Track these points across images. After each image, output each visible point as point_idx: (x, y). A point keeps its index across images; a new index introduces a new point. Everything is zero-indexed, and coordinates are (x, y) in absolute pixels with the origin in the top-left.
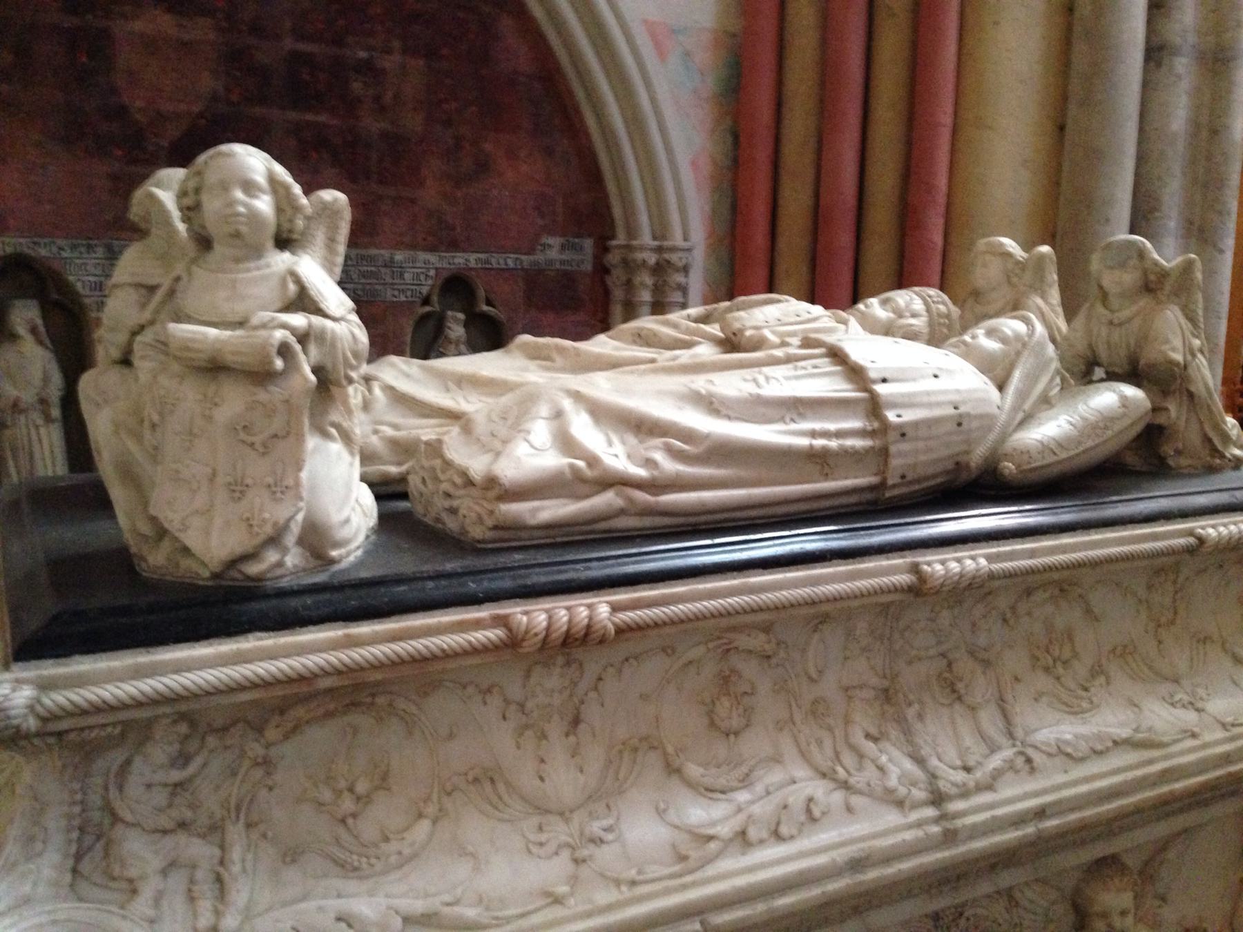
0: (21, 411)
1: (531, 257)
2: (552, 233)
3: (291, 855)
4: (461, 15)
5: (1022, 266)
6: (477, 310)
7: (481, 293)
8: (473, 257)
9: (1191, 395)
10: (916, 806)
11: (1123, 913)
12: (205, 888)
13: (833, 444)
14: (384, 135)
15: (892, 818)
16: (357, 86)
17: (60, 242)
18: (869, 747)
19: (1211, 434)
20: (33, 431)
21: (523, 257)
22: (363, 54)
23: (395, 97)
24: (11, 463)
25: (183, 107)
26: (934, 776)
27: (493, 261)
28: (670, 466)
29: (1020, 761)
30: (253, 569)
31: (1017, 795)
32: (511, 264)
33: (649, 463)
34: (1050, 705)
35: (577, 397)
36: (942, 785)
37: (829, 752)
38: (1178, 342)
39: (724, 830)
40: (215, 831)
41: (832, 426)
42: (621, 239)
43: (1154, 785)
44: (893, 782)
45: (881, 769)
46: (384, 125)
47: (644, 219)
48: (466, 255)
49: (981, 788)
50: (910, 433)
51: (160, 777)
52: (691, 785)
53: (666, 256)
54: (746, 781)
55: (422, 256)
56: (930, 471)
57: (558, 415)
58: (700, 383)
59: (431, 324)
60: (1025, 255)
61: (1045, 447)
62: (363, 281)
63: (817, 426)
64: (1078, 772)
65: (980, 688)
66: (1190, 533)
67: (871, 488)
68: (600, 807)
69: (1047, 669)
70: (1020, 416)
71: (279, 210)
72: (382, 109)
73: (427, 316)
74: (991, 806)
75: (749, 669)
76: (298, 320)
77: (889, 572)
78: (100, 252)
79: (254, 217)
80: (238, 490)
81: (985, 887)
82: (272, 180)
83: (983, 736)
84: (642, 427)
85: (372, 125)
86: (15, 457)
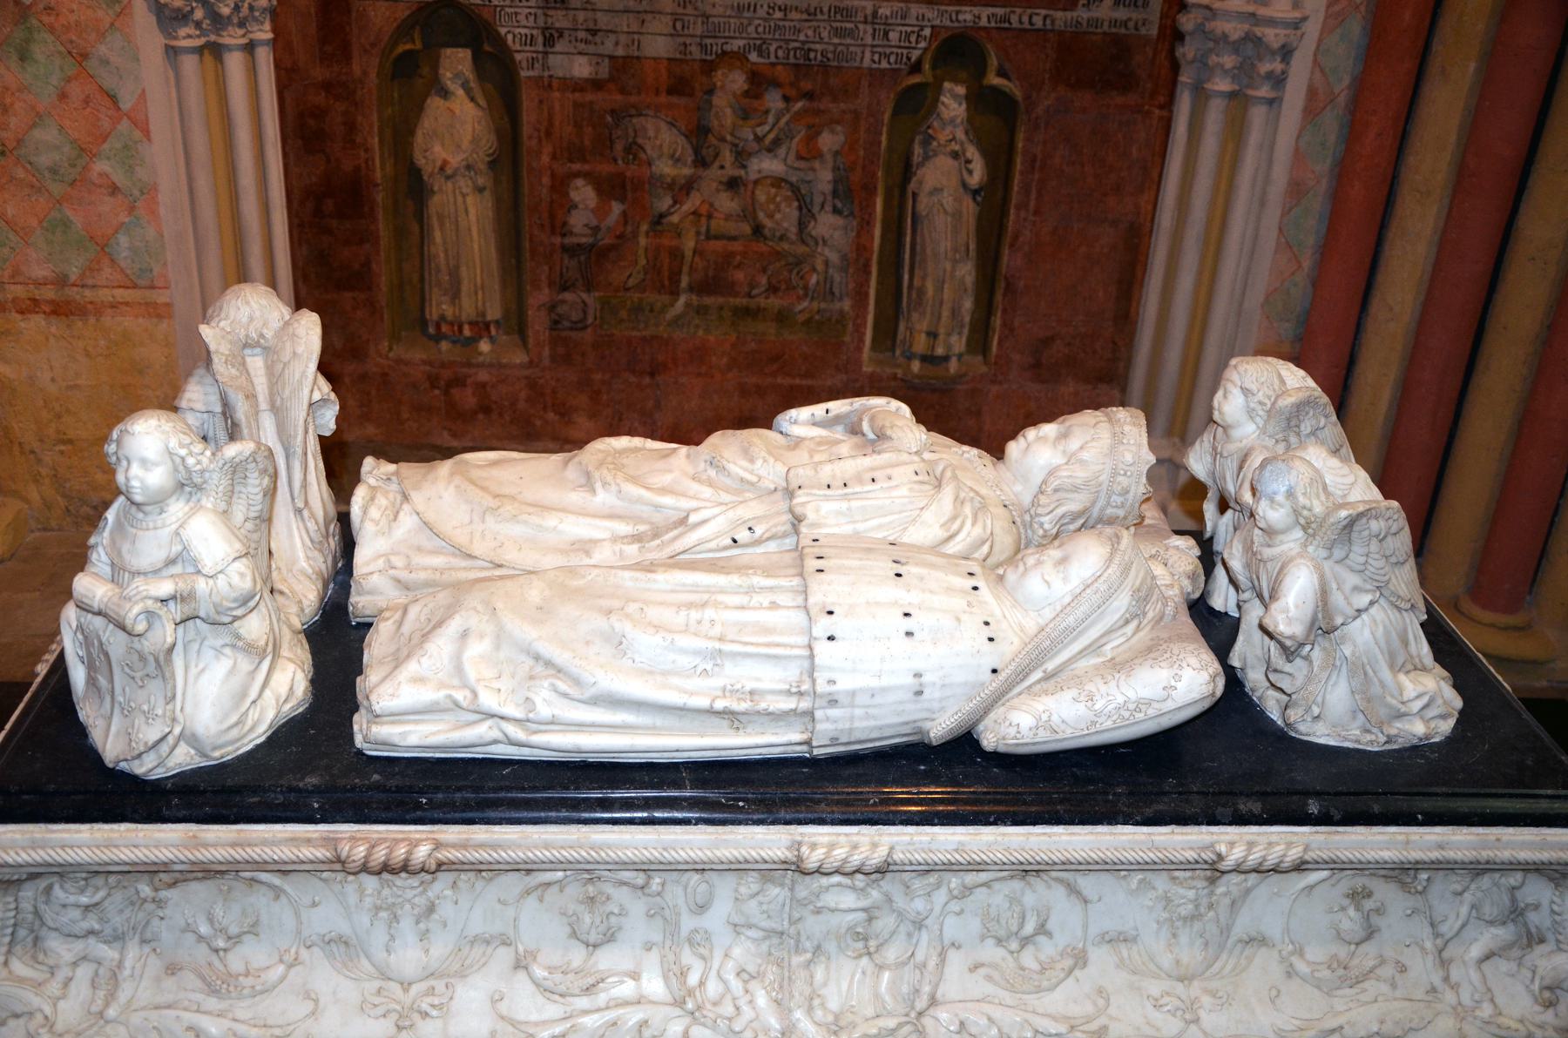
0: (448, 178)
1: (1069, 14)
6: (985, 82)
7: (993, 62)
20: (460, 199)
21: (1059, 14)
27: (1014, 19)
32: (1038, 22)
48: (976, 10)
53: (1258, 31)
55: (916, 10)
62: (836, 41)
86: (442, 225)
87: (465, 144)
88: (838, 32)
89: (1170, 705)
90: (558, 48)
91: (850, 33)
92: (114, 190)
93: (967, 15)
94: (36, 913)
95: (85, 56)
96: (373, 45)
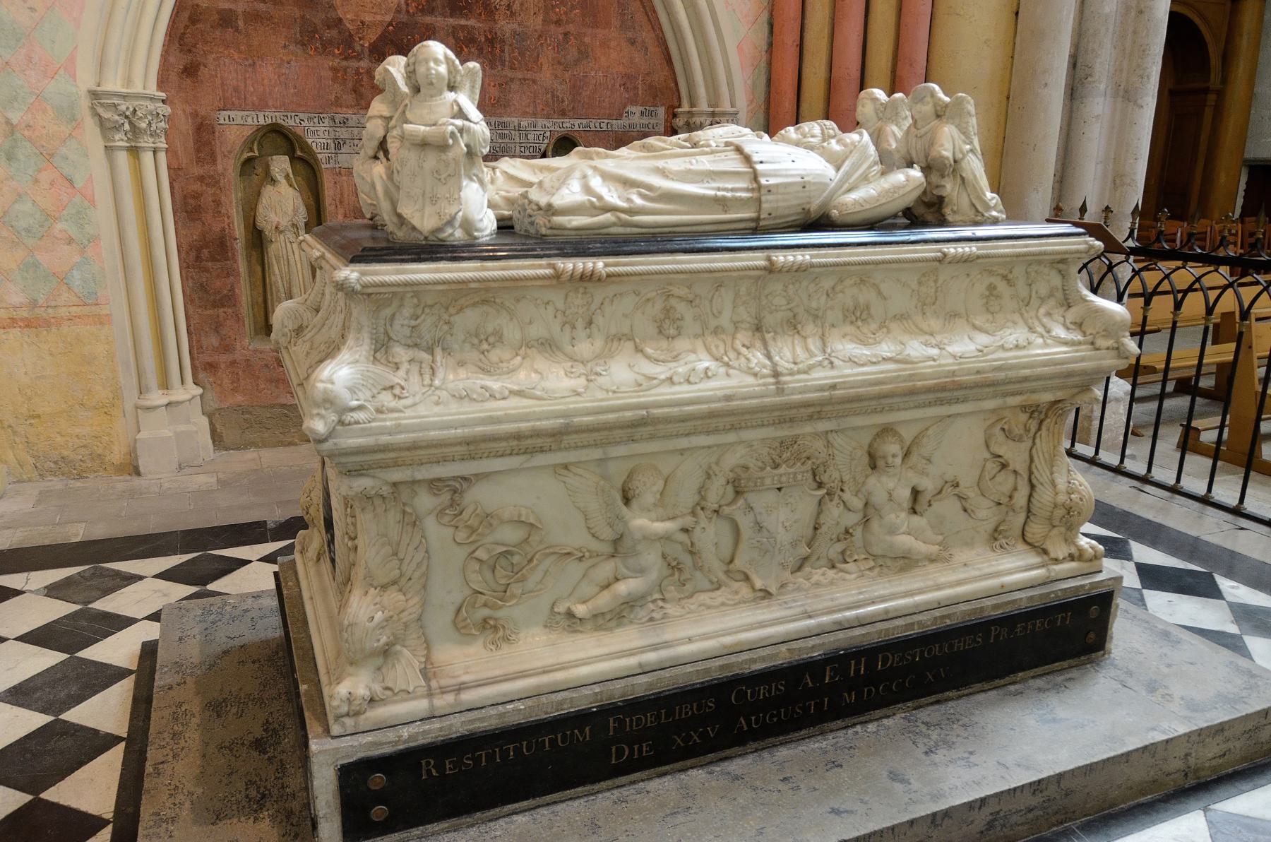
0: (281, 232)
2: (634, 102)
3: (461, 364)
5: (885, 106)
9: (963, 179)
10: (764, 377)
11: (894, 456)
12: (427, 370)
13: (729, 195)
14: (515, 33)
15: (751, 380)
17: (301, 115)
18: (744, 350)
19: (975, 201)
23: (522, 4)
24: (276, 268)
25: (379, 18)
26: (775, 365)
27: (592, 125)
28: (639, 201)
29: (826, 363)
30: (442, 236)
31: (821, 376)
33: (629, 200)
35: (595, 169)
36: (779, 369)
37: (722, 351)
38: (949, 146)
39: (663, 377)
40: (430, 350)
41: (730, 186)
42: (686, 107)
44: (752, 365)
45: (748, 359)
46: (515, 26)
47: (701, 91)
48: (572, 121)
49: (799, 372)
50: (774, 190)
51: (406, 322)
52: (648, 357)
54: (676, 358)
55: (541, 122)
56: (787, 212)
57: (585, 177)
58: (660, 164)
60: (886, 98)
61: (856, 202)
63: (721, 185)
65: (810, 329)
66: (940, 251)
67: (752, 220)
68: (602, 362)
69: (852, 323)
70: (846, 186)
71: (449, 72)
72: (513, 14)
74: (807, 380)
76: (459, 122)
77: (758, 260)
79: (438, 74)
80: (434, 200)
81: (808, 429)
82: (446, 57)
83: (807, 349)
84: (628, 183)
85: (505, 26)
86: (278, 263)
87: (290, 212)
89: (908, 189)
90: (343, 150)
91: (508, 136)
92: (70, 241)
94: (386, 333)
95: (52, 155)
96: (230, 152)
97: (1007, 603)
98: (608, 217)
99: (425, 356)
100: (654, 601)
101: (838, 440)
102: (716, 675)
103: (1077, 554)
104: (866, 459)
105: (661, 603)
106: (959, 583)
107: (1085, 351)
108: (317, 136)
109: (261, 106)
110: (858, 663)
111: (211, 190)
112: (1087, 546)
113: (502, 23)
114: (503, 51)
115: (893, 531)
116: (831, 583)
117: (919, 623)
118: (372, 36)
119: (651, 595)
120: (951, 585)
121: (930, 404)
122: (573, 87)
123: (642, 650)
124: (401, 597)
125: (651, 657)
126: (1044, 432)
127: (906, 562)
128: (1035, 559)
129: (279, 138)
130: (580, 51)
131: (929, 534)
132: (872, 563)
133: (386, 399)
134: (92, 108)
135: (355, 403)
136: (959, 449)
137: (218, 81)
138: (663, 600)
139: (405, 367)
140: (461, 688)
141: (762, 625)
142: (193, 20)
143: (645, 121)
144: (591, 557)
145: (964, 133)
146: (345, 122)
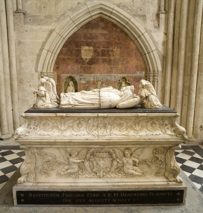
2: (138, 71)
4: (125, 42)
8: (126, 75)
12: (35, 130)
14: (114, 59)
15: (92, 137)
16: (110, 53)
18: (93, 131)
22: (111, 49)
23: (115, 54)
25: (89, 57)
28: (77, 104)
31: (108, 137)
32: (131, 75)
33: (75, 103)
34: (118, 131)
39: (75, 134)
41: (95, 101)
43: (127, 140)
46: (114, 58)
49: (103, 136)
52: (74, 131)
55: (119, 75)
59: (120, 84)
64: (118, 136)
72: (114, 56)
73: (119, 83)
75: (82, 122)
78: (79, 75)
84: (76, 100)
85: (112, 58)
88: (110, 77)
93: (124, 75)
97: (154, 188)
98: (71, 106)
99: (36, 127)
100: (77, 174)
101: (116, 150)
102: (85, 190)
103: (176, 181)
104: (122, 154)
105: (78, 175)
106: (144, 182)
107: (175, 137)
108: (77, 78)
109: (68, 73)
110: (116, 194)
111: (59, 87)
112: (178, 179)
113: (111, 57)
114: (111, 62)
115: (128, 169)
116: (115, 177)
117: (132, 188)
118: (88, 61)
119: (76, 173)
120: (142, 182)
121: (135, 144)
122: (125, 68)
123: (72, 183)
124: (31, 166)
125: (73, 184)
126: (168, 153)
127: (132, 175)
128: (166, 180)
129: (72, 79)
130: (127, 62)
131: (139, 170)
132: (125, 174)
133: (27, 134)
134: (41, 74)
135: (21, 134)
136: (147, 154)
137: (62, 69)
138: (79, 174)
139: (32, 129)
140: (38, 183)
141: (97, 183)
142: (59, 60)
143: (140, 74)
144: (64, 164)
145: (149, 91)
146: (82, 75)
